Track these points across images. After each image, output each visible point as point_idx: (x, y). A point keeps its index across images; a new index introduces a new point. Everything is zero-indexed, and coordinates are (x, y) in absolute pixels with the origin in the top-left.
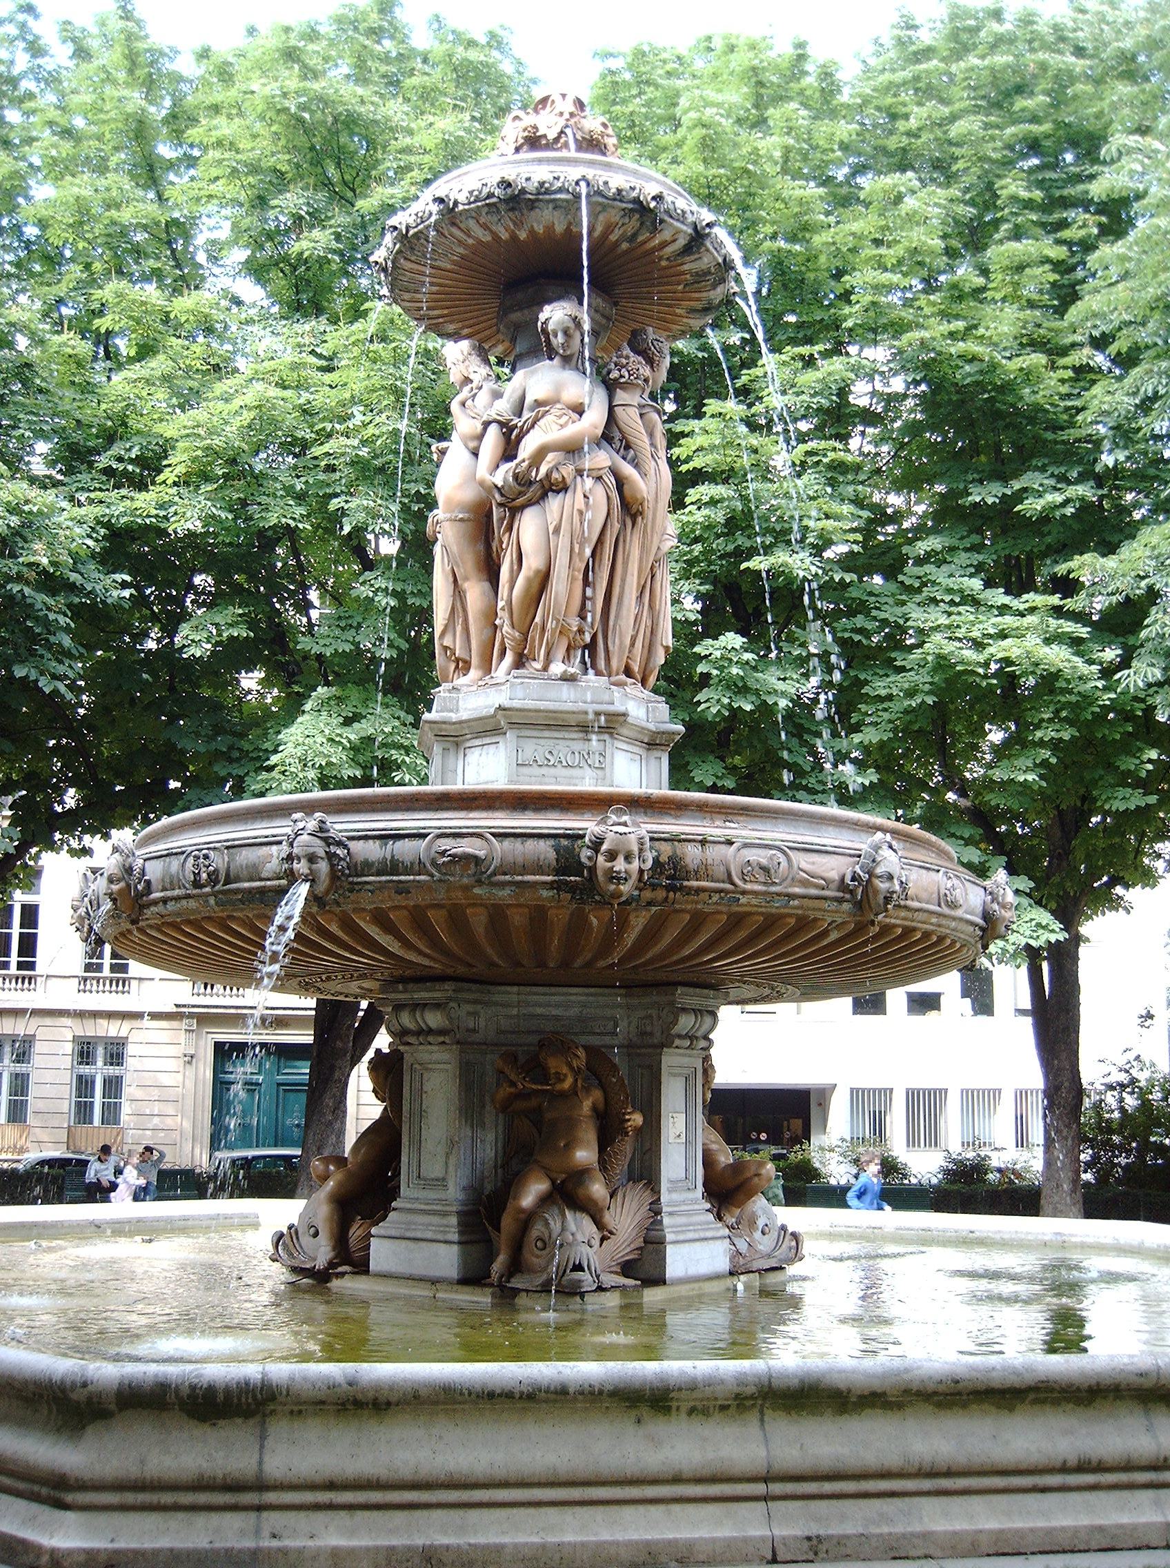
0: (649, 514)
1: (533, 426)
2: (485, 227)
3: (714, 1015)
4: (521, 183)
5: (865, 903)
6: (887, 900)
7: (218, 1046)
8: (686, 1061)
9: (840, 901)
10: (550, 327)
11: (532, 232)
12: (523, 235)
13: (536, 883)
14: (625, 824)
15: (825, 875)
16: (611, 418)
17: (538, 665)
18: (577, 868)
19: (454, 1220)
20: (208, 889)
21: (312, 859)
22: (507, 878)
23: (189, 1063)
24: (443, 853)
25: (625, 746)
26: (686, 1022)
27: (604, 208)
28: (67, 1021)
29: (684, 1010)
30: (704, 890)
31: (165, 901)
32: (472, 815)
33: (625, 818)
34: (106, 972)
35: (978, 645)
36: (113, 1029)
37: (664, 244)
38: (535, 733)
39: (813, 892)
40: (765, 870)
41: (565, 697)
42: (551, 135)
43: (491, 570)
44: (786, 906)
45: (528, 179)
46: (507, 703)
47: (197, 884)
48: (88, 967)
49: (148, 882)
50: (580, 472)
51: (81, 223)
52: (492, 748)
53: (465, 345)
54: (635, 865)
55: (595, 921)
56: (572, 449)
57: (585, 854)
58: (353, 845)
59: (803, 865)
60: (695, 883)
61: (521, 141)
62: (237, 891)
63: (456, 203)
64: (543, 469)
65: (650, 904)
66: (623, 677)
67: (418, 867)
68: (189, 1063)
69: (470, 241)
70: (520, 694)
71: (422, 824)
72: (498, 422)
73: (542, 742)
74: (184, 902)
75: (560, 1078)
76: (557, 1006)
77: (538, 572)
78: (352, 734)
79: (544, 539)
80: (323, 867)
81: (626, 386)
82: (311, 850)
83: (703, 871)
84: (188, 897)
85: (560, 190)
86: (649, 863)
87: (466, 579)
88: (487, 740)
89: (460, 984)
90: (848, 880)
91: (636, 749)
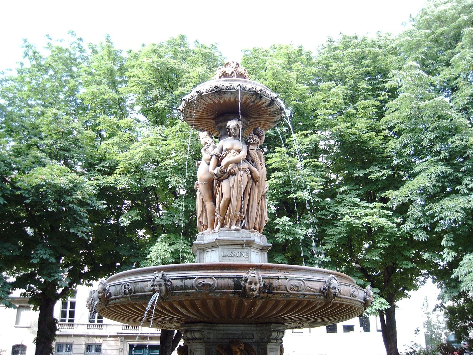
0: (260, 181)
2: (211, 99)
3: (283, 333)
4: (221, 87)
5: (328, 296)
6: (334, 295)
7: (131, 347)
8: (275, 347)
9: (320, 296)
10: (230, 127)
11: (224, 100)
12: (222, 101)
13: (228, 292)
14: (254, 274)
15: (315, 288)
16: (248, 153)
17: (228, 227)
18: (240, 287)
20: (128, 295)
21: (160, 285)
22: (219, 290)
23: (121, 351)
24: (200, 283)
25: (254, 250)
26: (274, 335)
27: (245, 93)
28: (83, 338)
29: (274, 331)
30: (279, 293)
31: (115, 299)
32: (208, 272)
33: (254, 272)
34: (96, 323)
35: (359, 218)
36: (98, 341)
37: (263, 104)
38: (227, 247)
39: (312, 293)
40: (297, 287)
41: (236, 236)
42: (230, 73)
43: (213, 198)
44: (303, 298)
45: (223, 86)
46: (219, 238)
47: (125, 293)
48: (91, 321)
49: (110, 293)
50: (240, 170)
51: (94, 99)
53: (205, 133)
54: (258, 286)
55: (246, 303)
56: (237, 163)
57: (243, 283)
58: (172, 281)
59: (309, 285)
60: (276, 291)
61: (221, 75)
62: (138, 295)
63: (202, 93)
64: (229, 169)
65: (262, 298)
66: (253, 230)
67: (192, 288)
68: (121, 351)
69: (207, 103)
70: (222, 235)
71: (193, 274)
72: (214, 155)
73: (229, 249)
74: (121, 299)
76: (236, 330)
77: (227, 199)
78: (172, 249)
79: (229, 189)
80: (163, 288)
81: (252, 144)
82: (160, 283)
83: (278, 288)
84: (122, 297)
85: (232, 89)
86: (262, 285)
87: (206, 201)
88: (213, 249)
90: (322, 289)
91: (257, 251)
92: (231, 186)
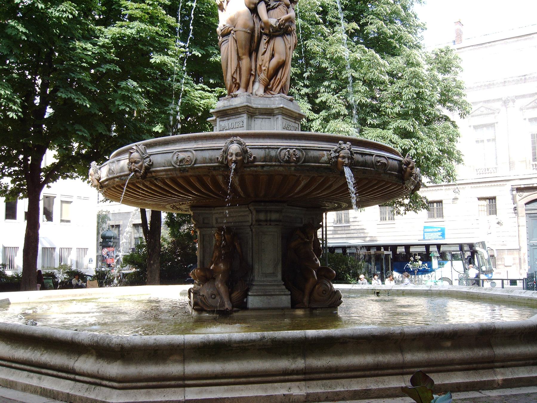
1: (276, 8)
19: (284, 287)
24: (379, 162)
31: (263, 166)
52: (267, 120)
62: (309, 166)
74: (276, 168)
87: (244, 54)
88: (266, 117)
92: (288, 46)
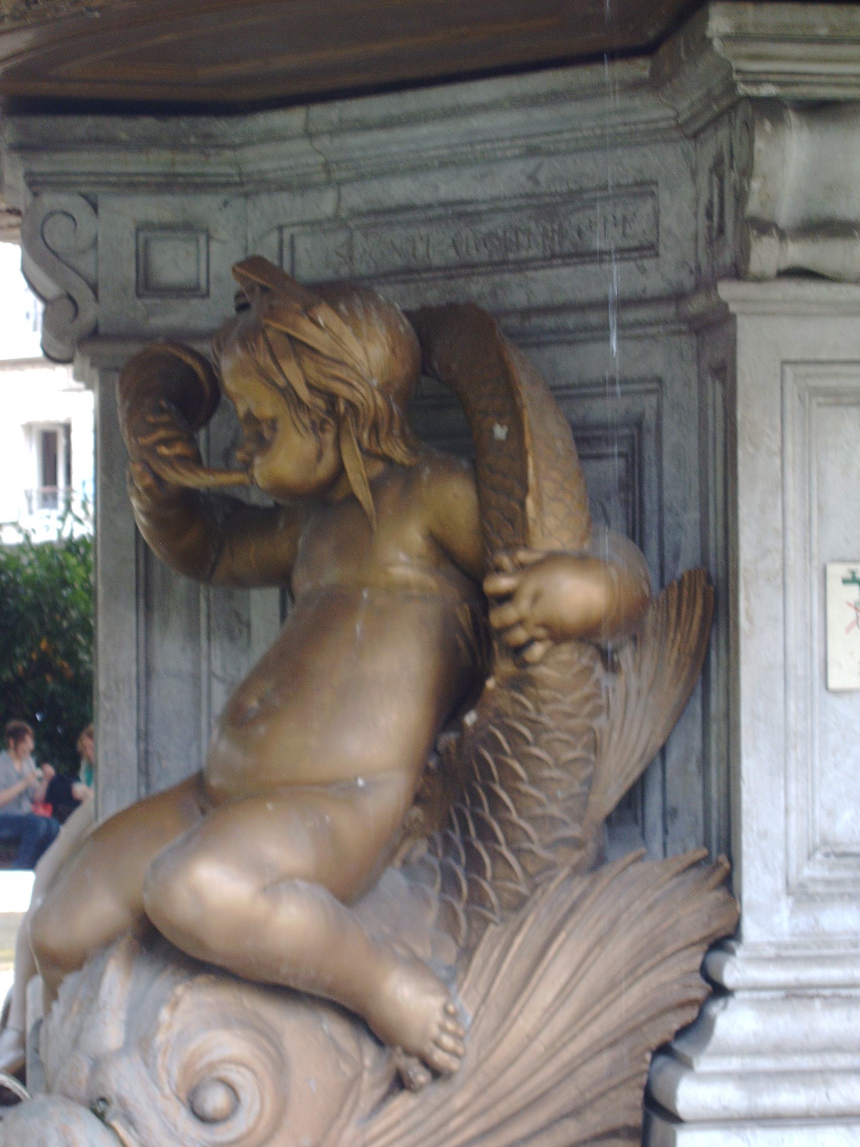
29: (771, 109)
75: (261, 434)
76: (447, 164)
89: (41, 124)
